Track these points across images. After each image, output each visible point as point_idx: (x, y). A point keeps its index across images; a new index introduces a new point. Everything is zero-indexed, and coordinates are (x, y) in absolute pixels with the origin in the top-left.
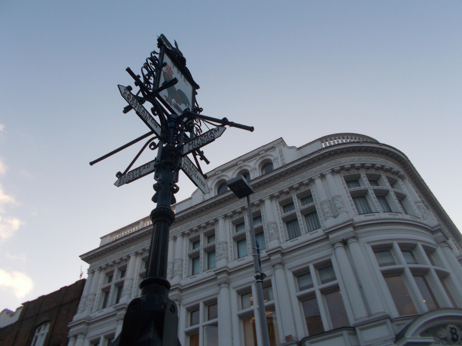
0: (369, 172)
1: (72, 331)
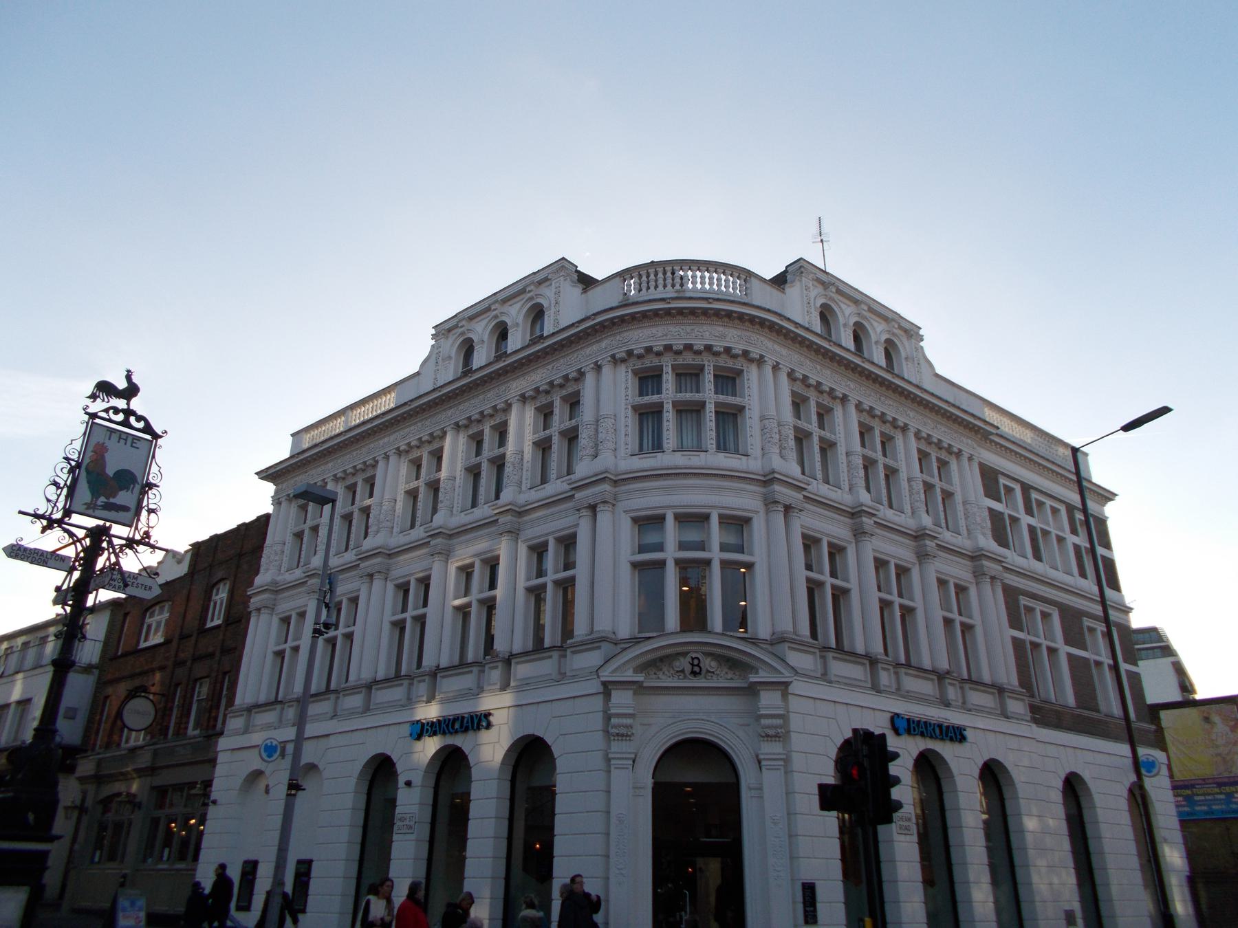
0: (680, 360)
1: (255, 602)
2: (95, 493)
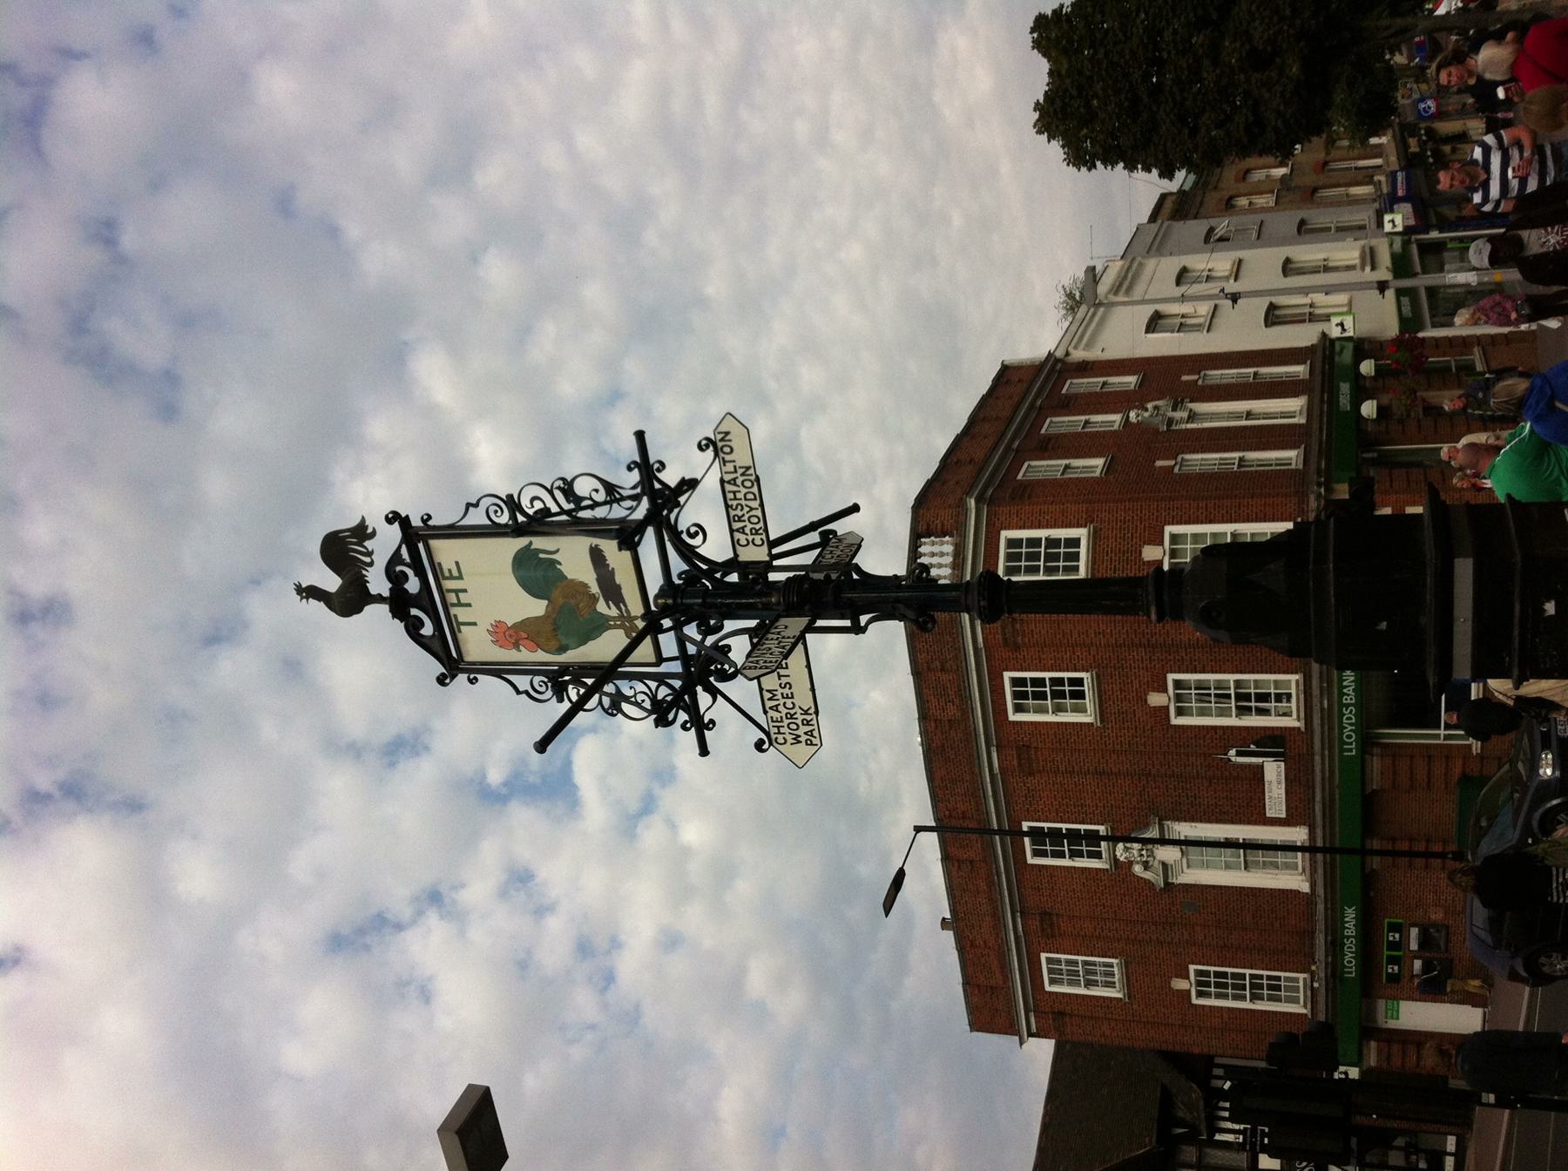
2: (599, 625)
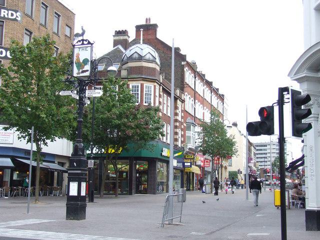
2: (79, 70)
